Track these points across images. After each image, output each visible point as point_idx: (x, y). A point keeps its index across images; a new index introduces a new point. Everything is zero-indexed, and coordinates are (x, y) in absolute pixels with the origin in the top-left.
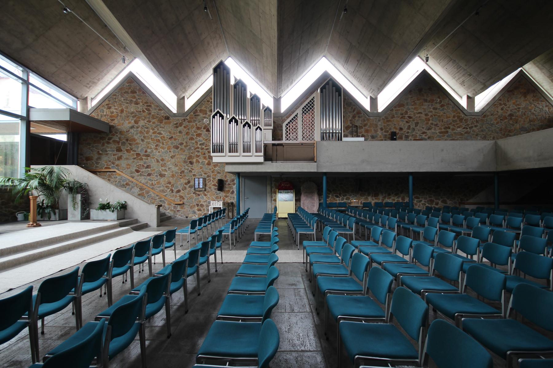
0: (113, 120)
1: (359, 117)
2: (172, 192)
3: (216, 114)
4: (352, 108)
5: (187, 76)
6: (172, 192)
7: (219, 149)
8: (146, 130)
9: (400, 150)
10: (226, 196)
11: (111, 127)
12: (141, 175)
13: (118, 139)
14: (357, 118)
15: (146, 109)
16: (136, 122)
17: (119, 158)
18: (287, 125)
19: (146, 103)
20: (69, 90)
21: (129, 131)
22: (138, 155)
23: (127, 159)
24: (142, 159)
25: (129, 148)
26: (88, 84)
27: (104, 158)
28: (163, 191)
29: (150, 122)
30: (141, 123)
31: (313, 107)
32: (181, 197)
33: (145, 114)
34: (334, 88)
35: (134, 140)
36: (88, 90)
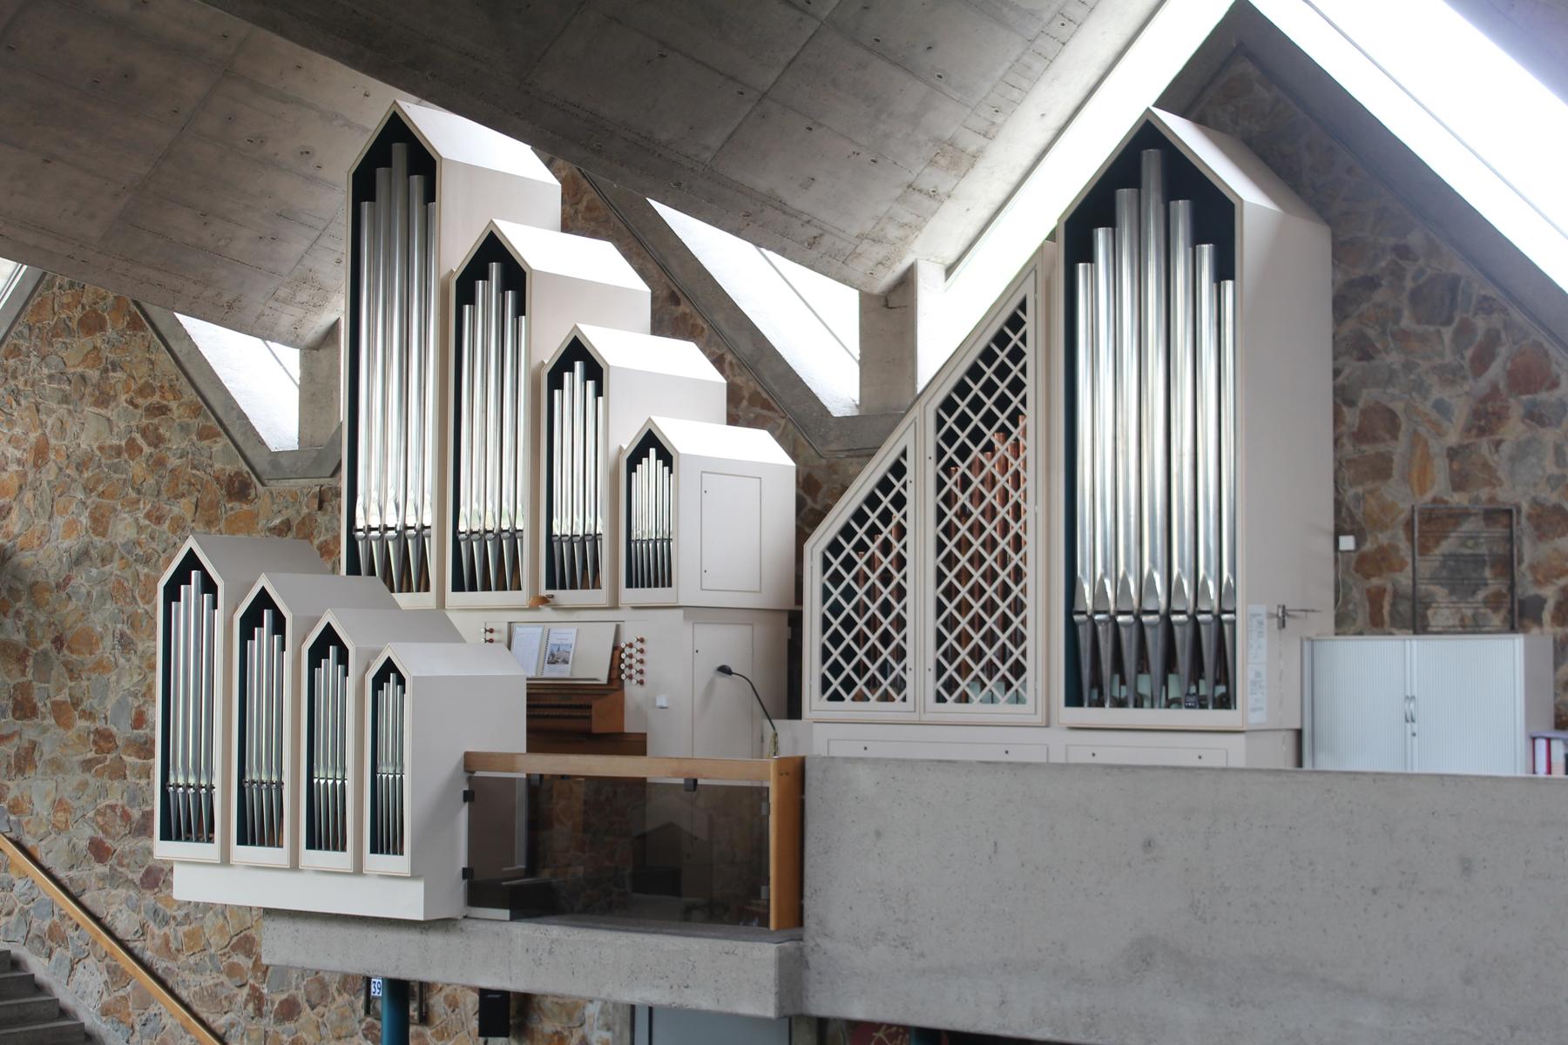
1: (1535, 417)
2: (259, 1012)
3: (181, 577)
4: (1465, 330)
5: (285, 215)
6: (259, 1012)
7: (188, 820)
8: (144, 570)
9: (1467, 867)
12: (113, 879)
13: (20, 638)
14: (1514, 430)
15: (144, 432)
16: (100, 523)
18: (835, 548)
21: (68, 579)
22: (104, 739)
23: (57, 765)
24: (119, 772)
25: (63, 696)
28: (213, 996)
29: (159, 520)
30: (123, 529)
31: (1017, 386)
33: (137, 468)
34: (1182, 210)
35: (89, 640)
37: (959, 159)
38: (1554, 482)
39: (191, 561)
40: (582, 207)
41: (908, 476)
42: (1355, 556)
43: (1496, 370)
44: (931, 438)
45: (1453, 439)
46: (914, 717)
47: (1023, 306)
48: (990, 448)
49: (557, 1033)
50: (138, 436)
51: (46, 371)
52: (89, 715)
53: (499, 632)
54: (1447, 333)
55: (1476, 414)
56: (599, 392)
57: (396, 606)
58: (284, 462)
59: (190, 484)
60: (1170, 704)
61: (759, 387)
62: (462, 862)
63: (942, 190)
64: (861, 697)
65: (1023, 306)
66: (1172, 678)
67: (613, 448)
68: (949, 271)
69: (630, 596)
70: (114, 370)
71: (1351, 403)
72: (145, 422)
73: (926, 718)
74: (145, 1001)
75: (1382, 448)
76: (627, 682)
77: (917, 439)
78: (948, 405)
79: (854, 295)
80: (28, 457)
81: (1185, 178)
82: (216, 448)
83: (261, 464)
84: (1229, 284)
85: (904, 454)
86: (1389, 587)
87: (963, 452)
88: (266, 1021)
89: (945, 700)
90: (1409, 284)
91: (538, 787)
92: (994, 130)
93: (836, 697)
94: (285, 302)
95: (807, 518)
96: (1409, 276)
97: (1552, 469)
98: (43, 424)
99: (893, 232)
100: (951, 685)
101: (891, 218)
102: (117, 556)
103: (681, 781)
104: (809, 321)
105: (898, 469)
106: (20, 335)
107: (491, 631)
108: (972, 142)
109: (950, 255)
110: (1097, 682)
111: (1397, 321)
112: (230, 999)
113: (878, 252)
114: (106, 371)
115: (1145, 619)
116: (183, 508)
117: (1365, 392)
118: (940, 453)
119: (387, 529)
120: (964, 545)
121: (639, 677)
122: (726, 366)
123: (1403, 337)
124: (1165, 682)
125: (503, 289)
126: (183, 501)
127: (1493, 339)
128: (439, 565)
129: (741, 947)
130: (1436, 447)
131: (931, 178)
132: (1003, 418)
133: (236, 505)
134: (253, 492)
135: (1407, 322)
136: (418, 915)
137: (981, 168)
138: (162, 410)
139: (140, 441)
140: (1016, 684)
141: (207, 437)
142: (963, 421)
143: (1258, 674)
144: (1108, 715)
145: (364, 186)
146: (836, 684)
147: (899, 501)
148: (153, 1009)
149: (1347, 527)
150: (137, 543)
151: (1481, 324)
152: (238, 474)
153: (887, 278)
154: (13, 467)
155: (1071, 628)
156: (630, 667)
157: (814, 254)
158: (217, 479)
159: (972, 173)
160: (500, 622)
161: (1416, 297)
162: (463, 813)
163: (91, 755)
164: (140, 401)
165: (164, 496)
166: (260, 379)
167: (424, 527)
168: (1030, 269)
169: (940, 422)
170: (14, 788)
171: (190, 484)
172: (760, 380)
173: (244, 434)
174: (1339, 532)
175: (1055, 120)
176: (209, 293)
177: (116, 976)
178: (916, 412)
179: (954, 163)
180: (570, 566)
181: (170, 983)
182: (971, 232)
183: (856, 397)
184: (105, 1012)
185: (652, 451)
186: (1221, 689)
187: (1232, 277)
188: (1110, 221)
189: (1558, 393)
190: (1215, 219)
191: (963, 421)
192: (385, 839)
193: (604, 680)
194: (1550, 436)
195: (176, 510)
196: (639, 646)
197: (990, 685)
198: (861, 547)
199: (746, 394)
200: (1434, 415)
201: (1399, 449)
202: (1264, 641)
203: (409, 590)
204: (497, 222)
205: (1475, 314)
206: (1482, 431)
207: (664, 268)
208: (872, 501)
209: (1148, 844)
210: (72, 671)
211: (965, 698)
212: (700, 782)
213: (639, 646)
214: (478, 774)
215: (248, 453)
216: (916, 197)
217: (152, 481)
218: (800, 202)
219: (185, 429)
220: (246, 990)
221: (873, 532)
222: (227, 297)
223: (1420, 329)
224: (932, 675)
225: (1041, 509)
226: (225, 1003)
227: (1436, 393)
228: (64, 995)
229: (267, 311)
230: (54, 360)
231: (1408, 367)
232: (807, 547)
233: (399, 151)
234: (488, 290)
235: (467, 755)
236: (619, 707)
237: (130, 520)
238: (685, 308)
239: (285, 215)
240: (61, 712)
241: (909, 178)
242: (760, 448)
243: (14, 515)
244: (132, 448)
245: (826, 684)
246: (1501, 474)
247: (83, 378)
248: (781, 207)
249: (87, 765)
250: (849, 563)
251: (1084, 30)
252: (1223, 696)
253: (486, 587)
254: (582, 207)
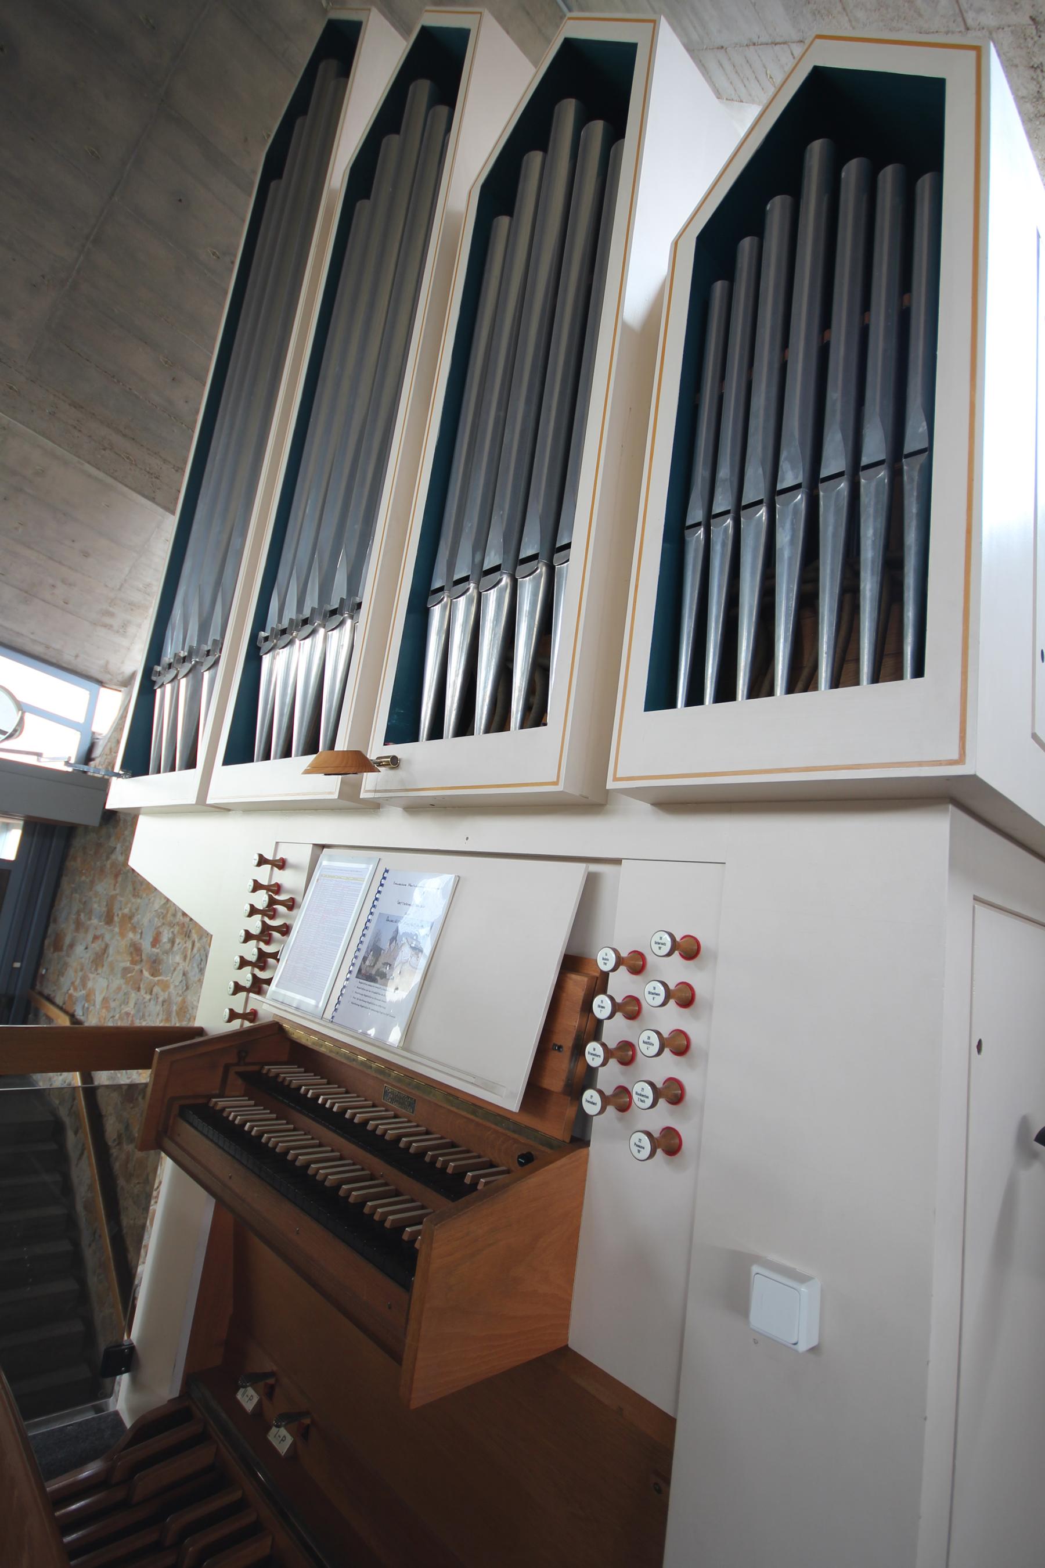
20: (38, 650)
26: (112, 615)
36: (125, 643)
53: (295, 867)
76: (604, 1124)
107: (281, 864)
156: (625, 1054)
163: (128, 964)
193: (507, 1092)
196: (676, 971)
213: (676, 971)
236: (560, 1234)
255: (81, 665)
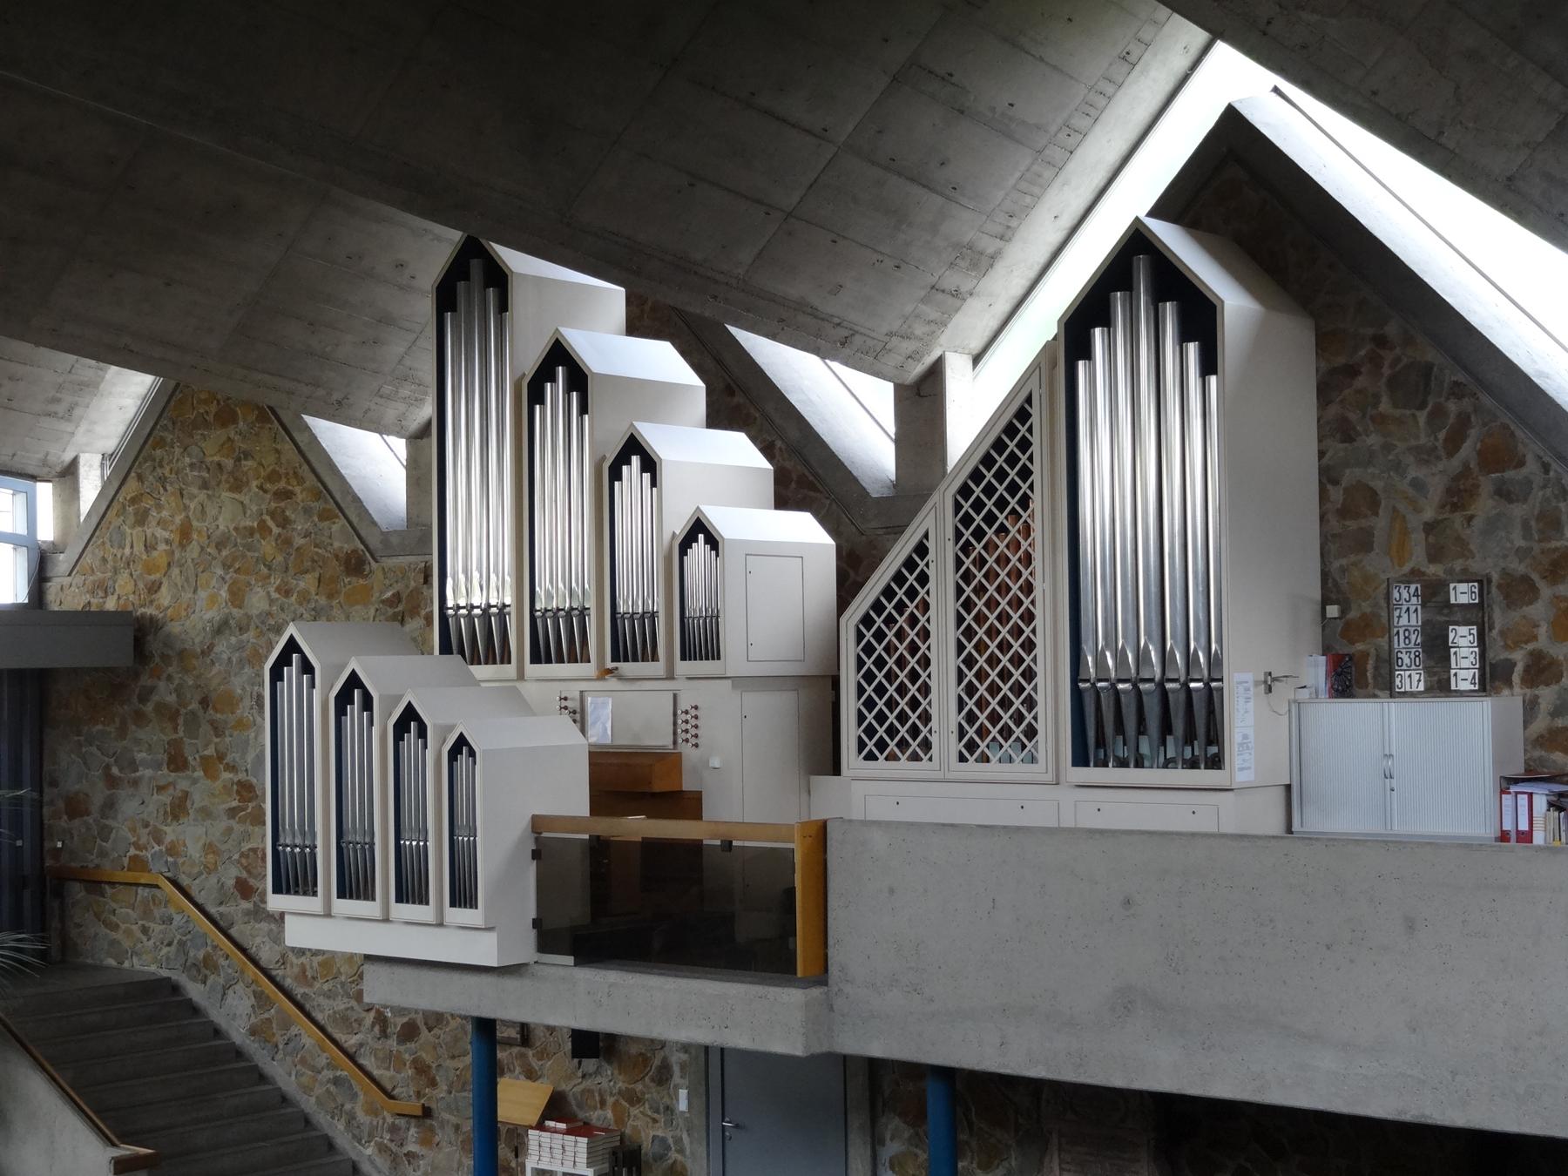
0: (154, 588)
3: (284, 660)
4: (1438, 414)
5: (386, 320)
6: (384, 1034)
7: (295, 877)
10: (634, 1099)
11: (141, 637)
13: (171, 699)
14: (1484, 506)
15: (272, 514)
16: (237, 597)
17: (178, 810)
18: (867, 621)
19: (273, 477)
21: (211, 647)
23: (206, 813)
25: (210, 751)
26: (59, 401)
27: (129, 807)
28: (345, 1020)
29: (287, 593)
30: (257, 601)
31: (1025, 473)
32: (421, 1069)
33: (267, 547)
34: (1169, 309)
35: (231, 702)
36: (69, 427)
37: (981, 261)
38: (1523, 554)
39: (292, 646)
40: (647, 308)
41: (931, 556)
42: (1341, 624)
43: (1468, 450)
44: (950, 521)
45: (1429, 514)
46: (940, 775)
47: (1029, 400)
48: (1003, 530)
49: (641, 1054)
50: (267, 518)
51: (187, 460)
52: (232, 768)
54: (1422, 416)
55: (1449, 491)
56: (654, 484)
57: (477, 683)
58: (394, 540)
59: (313, 561)
60: (1168, 764)
61: (803, 470)
62: (533, 914)
63: (964, 289)
64: (892, 757)
65: (1029, 400)
66: (1170, 739)
67: (667, 536)
68: (977, 360)
69: (684, 667)
70: (246, 459)
71: (1335, 482)
72: (273, 505)
73: (949, 776)
74: (286, 1024)
75: (1364, 523)
77: (936, 522)
78: (965, 491)
79: (888, 388)
80: (175, 537)
81: (1173, 283)
82: (335, 528)
83: (374, 542)
84: (1213, 379)
85: (926, 536)
86: (1373, 651)
87: (979, 534)
88: (390, 1042)
89: (967, 760)
90: (1386, 371)
91: (599, 848)
92: (1009, 233)
93: (871, 757)
94: (388, 398)
95: (847, 587)
96: (1387, 363)
97: (1520, 542)
98: (186, 508)
99: (919, 329)
100: (971, 746)
101: (917, 316)
102: (252, 627)
103: (718, 842)
104: (851, 409)
105: (921, 550)
106: (165, 428)
108: (990, 245)
109: (976, 345)
110: (1101, 742)
111: (1376, 405)
112: (359, 1022)
113: (908, 346)
114: (239, 460)
115: (1142, 686)
116: (307, 582)
117: (1348, 471)
118: (959, 535)
119: (473, 607)
120: (981, 619)
121: (694, 741)
122: (777, 452)
123: (1381, 420)
124: (1164, 743)
125: (569, 389)
126: (308, 576)
127: (1464, 422)
128: (519, 639)
129: (773, 992)
130: (1415, 521)
131: (951, 280)
132: (1013, 502)
133: (354, 579)
134: (367, 568)
135: (1385, 406)
136: (493, 962)
137: (1000, 268)
138: (286, 495)
139: (270, 523)
140: (1029, 745)
141: (327, 519)
142: (978, 506)
143: (1245, 737)
144: (1111, 774)
145: (446, 298)
146: (870, 745)
147: (923, 579)
148: (294, 1030)
149: (1334, 596)
150: (269, 614)
151: (1452, 407)
152: (355, 551)
153: (918, 369)
154: (162, 547)
155: (1077, 695)
157: (847, 351)
158: (337, 556)
159: (992, 273)
160: (573, 690)
161: (1393, 383)
162: (532, 868)
163: (235, 804)
164: (268, 486)
165: (291, 572)
166: (373, 462)
167: (505, 606)
168: (1035, 366)
169: (958, 507)
170: (171, 832)
171: (313, 561)
172: (806, 463)
173: (359, 515)
174: (1325, 601)
175: (1067, 221)
176: (321, 392)
177: (262, 1000)
178: (935, 498)
179: (974, 265)
180: (631, 643)
181: (308, 1007)
182: (994, 324)
183: (893, 478)
184: (253, 1032)
185: (701, 537)
186: (1213, 750)
187: (1215, 372)
188: (1106, 322)
189: (1524, 471)
190: (1199, 319)
191: (978, 506)
192: (463, 895)
194: (1518, 511)
195: (302, 584)
196: (693, 712)
197: (1006, 745)
198: (890, 621)
199: (794, 477)
200: (1411, 492)
201: (1380, 523)
202: (1251, 705)
203: (494, 662)
204: (562, 330)
205: (1448, 399)
206: (1455, 507)
207: (719, 361)
208: (899, 578)
209: (1128, 902)
210: (218, 730)
211: (985, 759)
212: (735, 843)
213: (693, 712)
214: (545, 835)
215: (363, 533)
216: (940, 296)
217: (280, 558)
218: (830, 306)
219: (307, 511)
220: (372, 1014)
221: (900, 607)
222: (336, 396)
223: (1397, 413)
224: (954, 737)
225: (1047, 586)
226: (355, 1025)
227: (1413, 472)
228: (217, 1015)
229: (373, 407)
230: (194, 450)
231: (1387, 448)
232: (843, 620)
233: (476, 266)
234: (555, 391)
235: (534, 817)
237: (262, 593)
238: (739, 399)
239: (386, 320)
240: (209, 766)
241: (933, 280)
242: (804, 530)
243: (164, 589)
244: (263, 529)
245: (861, 745)
246: (1472, 547)
247: (219, 465)
248: (814, 313)
249: (232, 813)
250: (879, 635)
251: (1090, 139)
252: (1216, 755)
253: (560, 660)
254: (647, 308)
255: (16, 464)
